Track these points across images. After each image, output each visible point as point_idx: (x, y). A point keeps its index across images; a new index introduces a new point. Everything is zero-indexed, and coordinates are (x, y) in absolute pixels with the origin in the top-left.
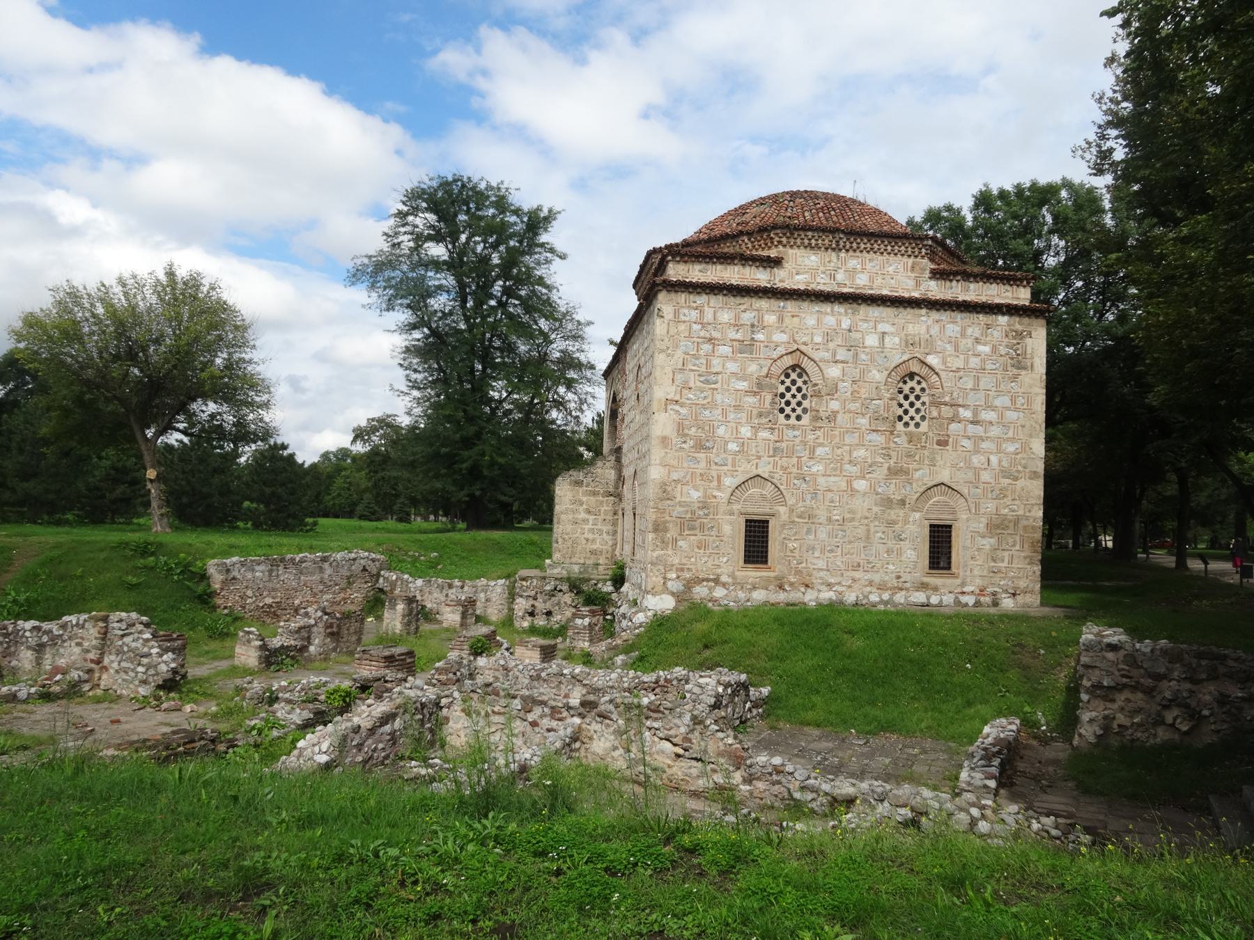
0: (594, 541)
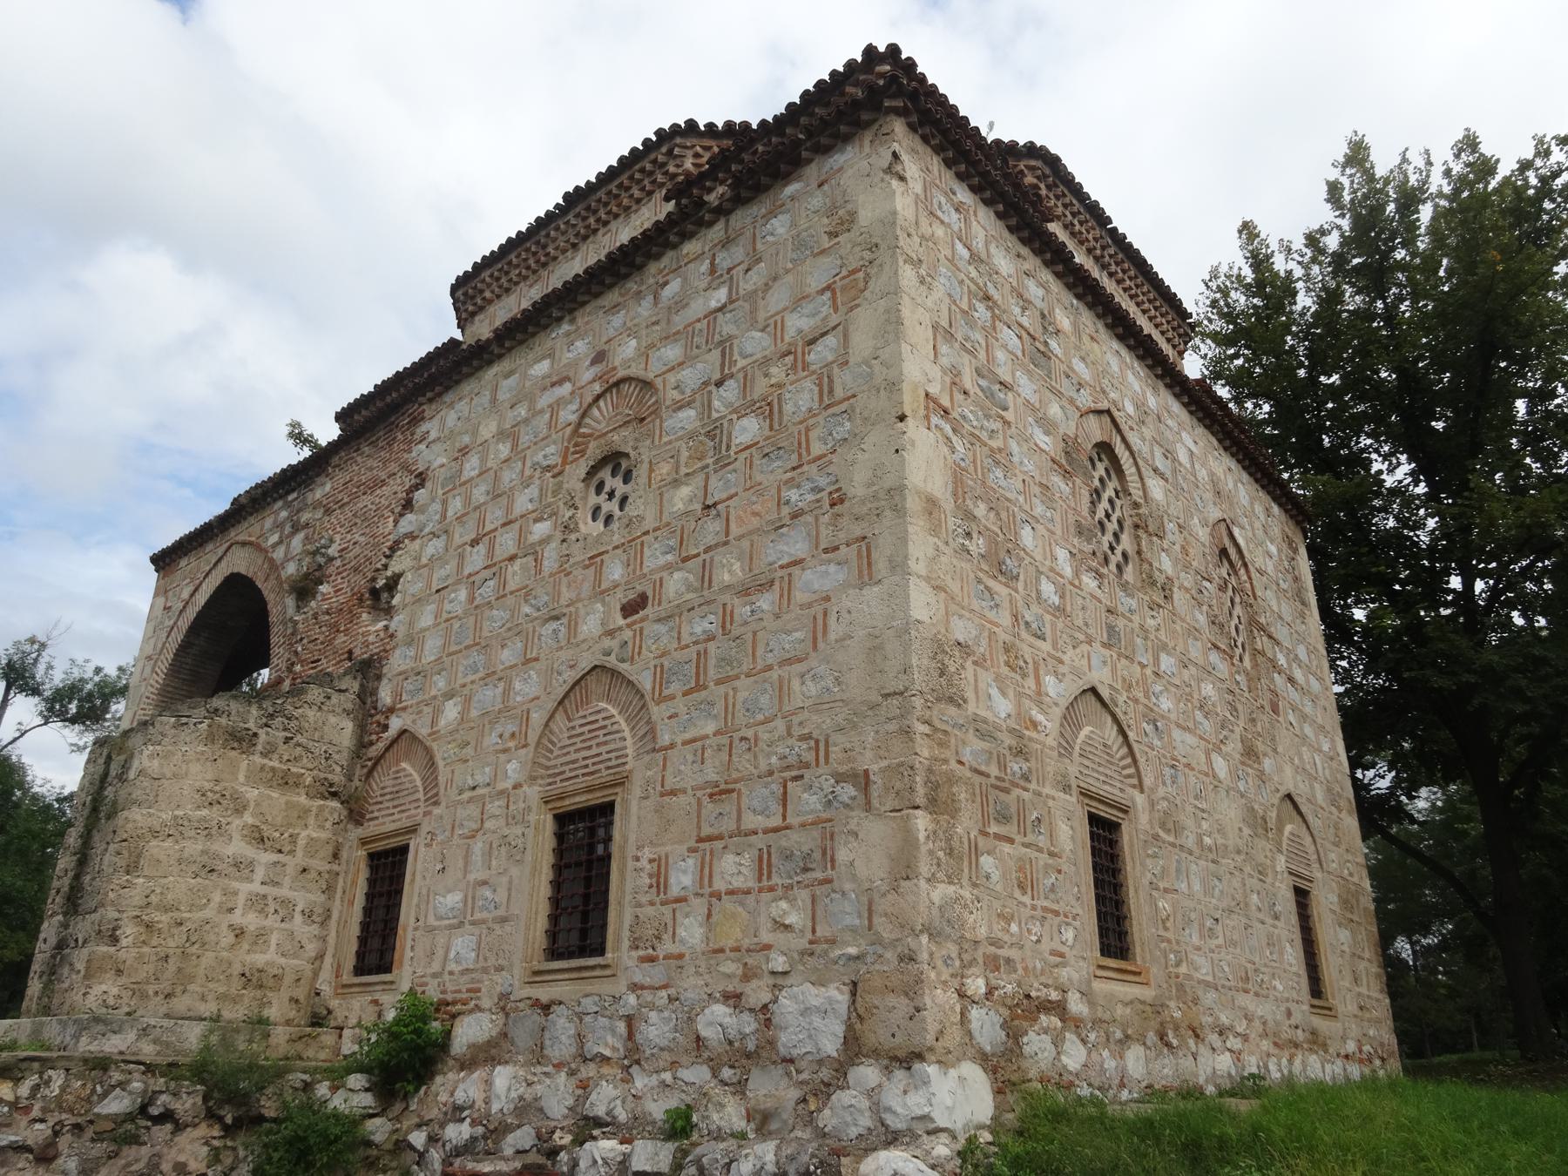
0: (261, 936)
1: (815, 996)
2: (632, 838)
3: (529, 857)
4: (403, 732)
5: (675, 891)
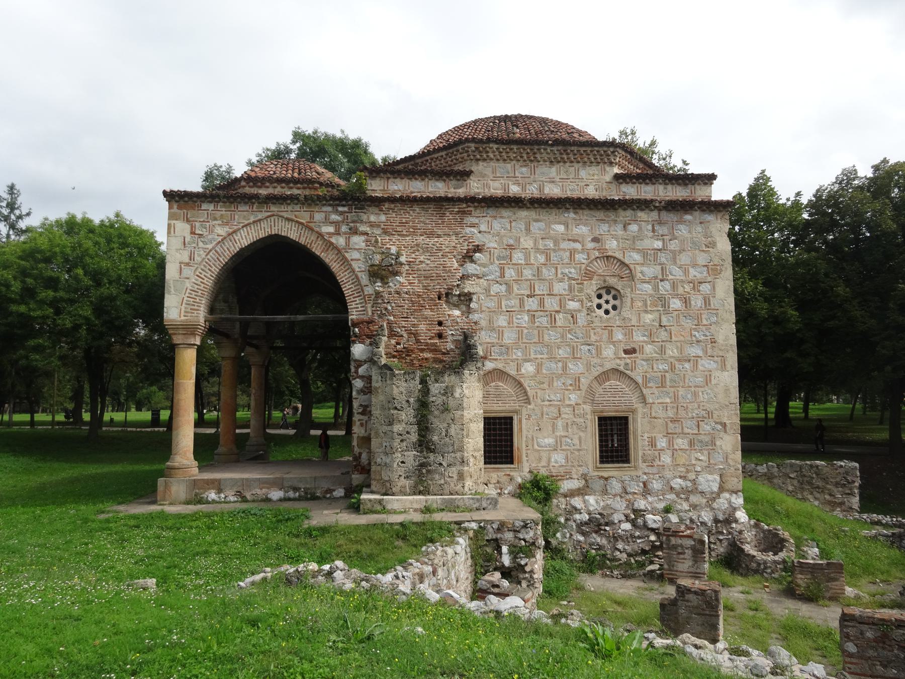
1: (710, 477)
2: (639, 430)
3: (589, 429)
4: (495, 370)
5: (659, 447)
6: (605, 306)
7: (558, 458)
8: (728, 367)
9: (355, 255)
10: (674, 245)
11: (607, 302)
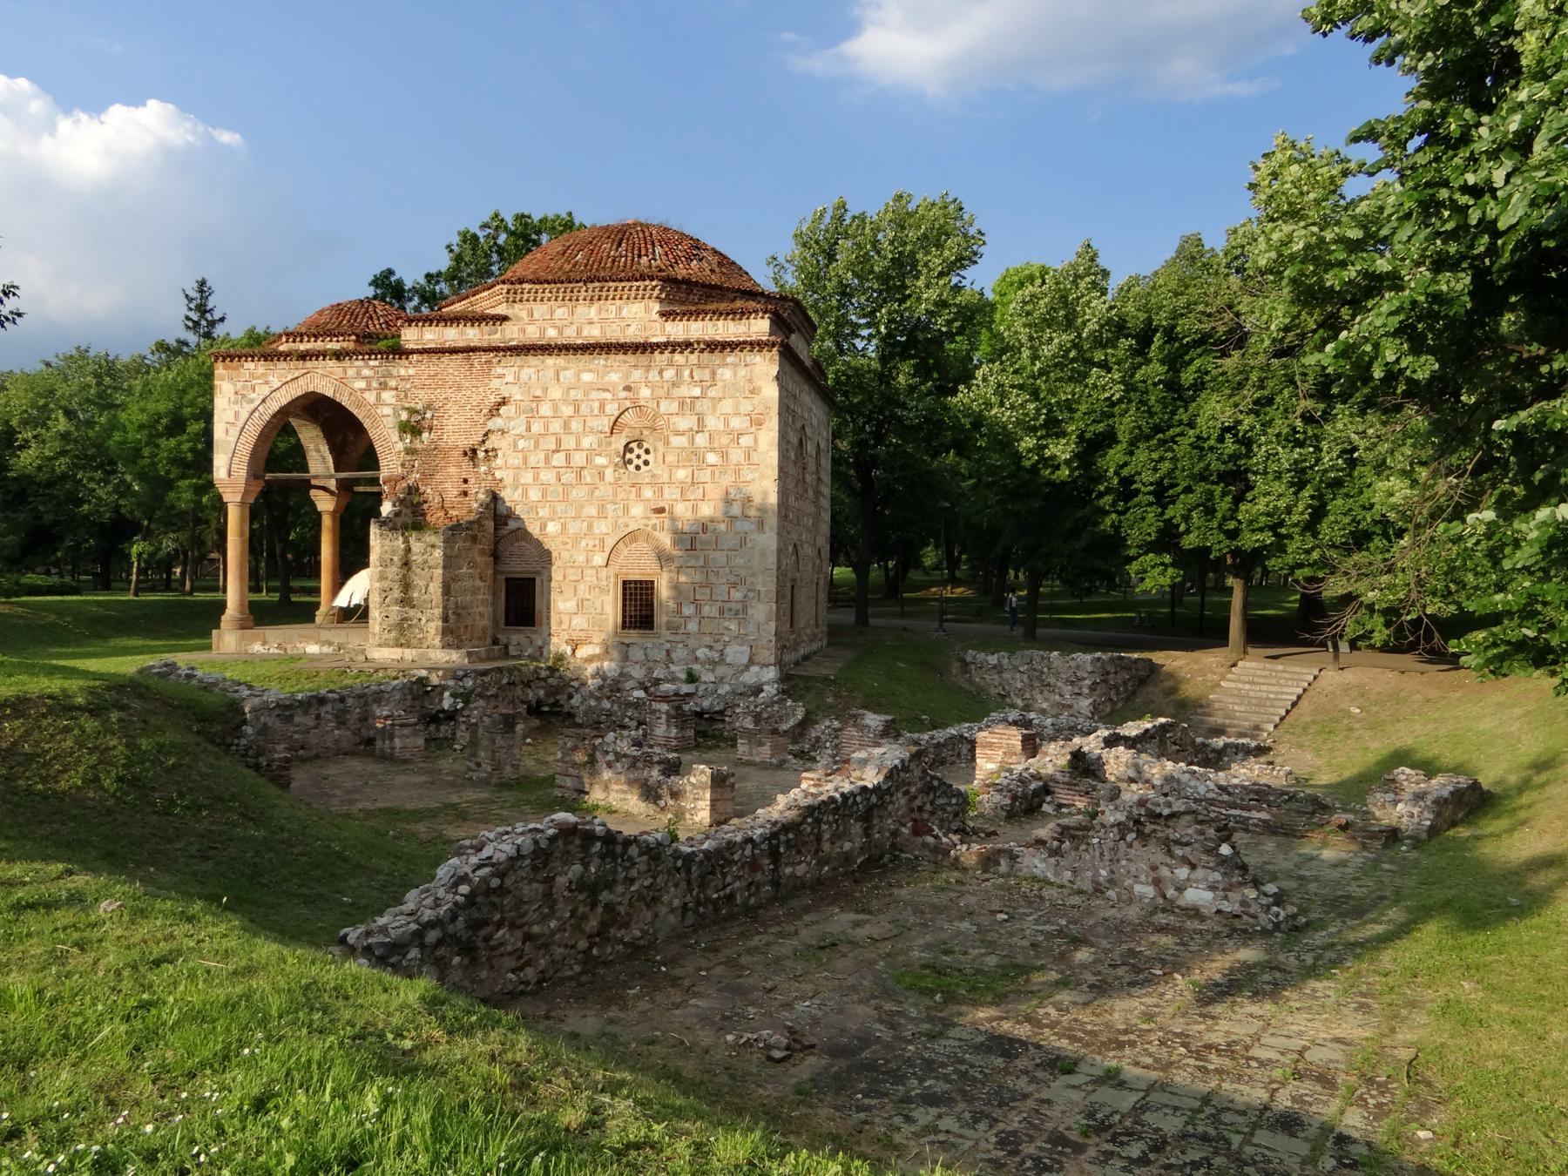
6: (636, 462)
7: (579, 622)
8: (767, 529)
9: (387, 411)
10: (712, 393)
11: (638, 457)
